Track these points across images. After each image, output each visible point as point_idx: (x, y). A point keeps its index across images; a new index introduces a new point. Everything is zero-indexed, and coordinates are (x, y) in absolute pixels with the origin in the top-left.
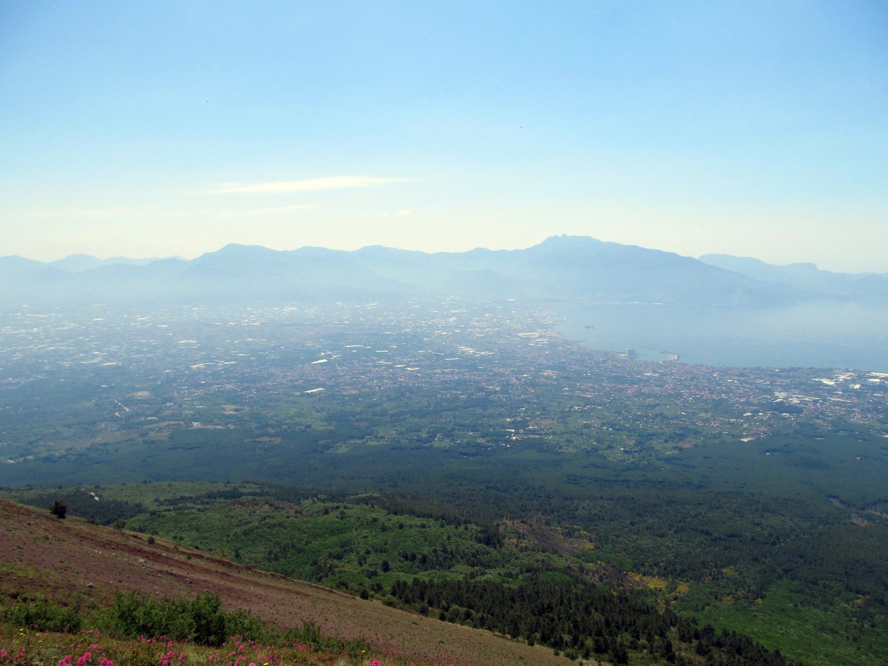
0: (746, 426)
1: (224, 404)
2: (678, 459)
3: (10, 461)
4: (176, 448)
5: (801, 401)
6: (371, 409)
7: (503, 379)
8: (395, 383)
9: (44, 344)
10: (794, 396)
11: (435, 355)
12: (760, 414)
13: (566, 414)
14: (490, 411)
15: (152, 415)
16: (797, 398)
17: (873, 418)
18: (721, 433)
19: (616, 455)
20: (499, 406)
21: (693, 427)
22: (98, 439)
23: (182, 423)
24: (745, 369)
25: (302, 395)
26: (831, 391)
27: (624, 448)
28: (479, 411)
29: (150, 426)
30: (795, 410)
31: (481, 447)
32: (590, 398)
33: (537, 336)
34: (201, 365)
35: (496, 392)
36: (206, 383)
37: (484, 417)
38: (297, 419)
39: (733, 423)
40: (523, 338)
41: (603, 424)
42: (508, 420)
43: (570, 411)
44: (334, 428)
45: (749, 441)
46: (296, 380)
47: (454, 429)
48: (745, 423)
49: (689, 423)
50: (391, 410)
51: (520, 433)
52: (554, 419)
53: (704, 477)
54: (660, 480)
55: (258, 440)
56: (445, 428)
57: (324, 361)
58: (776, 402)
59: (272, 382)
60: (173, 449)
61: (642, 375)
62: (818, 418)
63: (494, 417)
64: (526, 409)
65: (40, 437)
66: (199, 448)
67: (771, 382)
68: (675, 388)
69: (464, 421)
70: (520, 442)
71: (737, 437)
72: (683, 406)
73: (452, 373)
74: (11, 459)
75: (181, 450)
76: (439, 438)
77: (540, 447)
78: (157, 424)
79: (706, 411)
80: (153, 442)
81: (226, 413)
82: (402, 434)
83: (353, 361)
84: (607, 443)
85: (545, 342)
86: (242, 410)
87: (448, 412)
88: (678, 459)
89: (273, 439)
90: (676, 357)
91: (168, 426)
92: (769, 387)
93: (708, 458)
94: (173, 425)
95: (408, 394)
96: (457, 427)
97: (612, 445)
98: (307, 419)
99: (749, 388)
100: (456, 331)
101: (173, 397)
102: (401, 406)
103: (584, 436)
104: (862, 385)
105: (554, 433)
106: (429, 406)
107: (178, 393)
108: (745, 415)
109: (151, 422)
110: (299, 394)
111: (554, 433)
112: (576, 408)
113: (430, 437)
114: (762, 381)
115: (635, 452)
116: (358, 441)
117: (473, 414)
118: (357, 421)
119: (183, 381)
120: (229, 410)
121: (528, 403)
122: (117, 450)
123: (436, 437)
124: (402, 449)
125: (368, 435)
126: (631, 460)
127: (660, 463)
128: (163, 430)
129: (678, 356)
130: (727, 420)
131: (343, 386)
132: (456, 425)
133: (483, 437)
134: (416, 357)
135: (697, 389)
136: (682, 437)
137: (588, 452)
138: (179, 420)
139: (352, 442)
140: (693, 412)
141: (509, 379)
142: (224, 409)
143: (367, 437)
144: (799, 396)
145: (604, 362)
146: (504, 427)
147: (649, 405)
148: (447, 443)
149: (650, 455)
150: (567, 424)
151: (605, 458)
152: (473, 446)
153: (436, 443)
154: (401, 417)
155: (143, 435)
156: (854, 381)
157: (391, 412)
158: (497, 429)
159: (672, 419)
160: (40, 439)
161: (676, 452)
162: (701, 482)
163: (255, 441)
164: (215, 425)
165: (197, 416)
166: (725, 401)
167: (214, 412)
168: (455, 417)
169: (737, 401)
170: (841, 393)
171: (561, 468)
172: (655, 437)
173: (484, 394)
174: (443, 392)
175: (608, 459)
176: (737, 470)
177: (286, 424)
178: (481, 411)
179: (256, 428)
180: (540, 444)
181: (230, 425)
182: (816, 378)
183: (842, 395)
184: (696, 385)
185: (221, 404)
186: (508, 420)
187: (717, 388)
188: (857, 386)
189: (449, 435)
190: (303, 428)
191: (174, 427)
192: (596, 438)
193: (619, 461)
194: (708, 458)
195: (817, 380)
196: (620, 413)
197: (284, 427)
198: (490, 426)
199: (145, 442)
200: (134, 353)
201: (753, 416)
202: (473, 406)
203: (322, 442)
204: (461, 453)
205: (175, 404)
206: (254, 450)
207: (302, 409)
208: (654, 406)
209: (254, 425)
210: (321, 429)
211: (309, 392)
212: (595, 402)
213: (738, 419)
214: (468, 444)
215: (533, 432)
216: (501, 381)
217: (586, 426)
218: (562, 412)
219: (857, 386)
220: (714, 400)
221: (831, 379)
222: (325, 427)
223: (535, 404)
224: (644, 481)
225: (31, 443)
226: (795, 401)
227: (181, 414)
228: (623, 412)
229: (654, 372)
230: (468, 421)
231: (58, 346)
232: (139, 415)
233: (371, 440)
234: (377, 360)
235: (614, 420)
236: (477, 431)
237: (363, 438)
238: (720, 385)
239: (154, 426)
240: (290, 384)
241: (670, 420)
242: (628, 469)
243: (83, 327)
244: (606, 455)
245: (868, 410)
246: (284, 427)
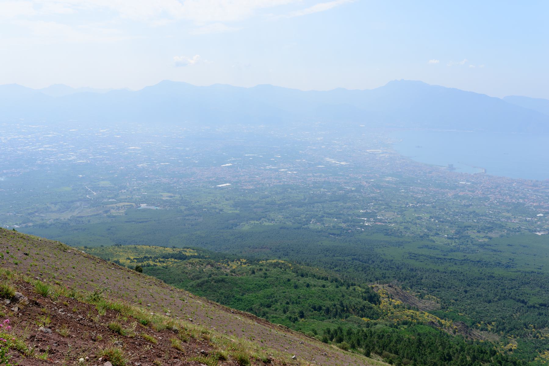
0: (539, 223)
1: (162, 192)
2: (488, 245)
3: (15, 226)
4: (130, 222)
6: (264, 200)
7: (356, 182)
8: (280, 182)
9: (36, 146)
11: (308, 163)
13: (404, 209)
14: (349, 204)
15: (113, 198)
18: (520, 227)
19: (441, 240)
20: (355, 201)
21: (499, 222)
22: (76, 213)
23: (134, 204)
24: (537, 181)
25: (216, 188)
27: (448, 235)
28: (341, 204)
29: (111, 205)
31: (344, 230)
32: (420, 198)
33: (380, 152)
34: (145, 165)
35: (352, 191)
36: (148, 177)
37: (344, 208)
38: (213, 205)
39: (529, 221)
40: (370, 153)
41: (431, 217)
42: (361, 211)
43: (406, 207)
44: (239, 212)
45: (542, 235)
46: (210, 177)
47: (323, 216)
49: (496, 219)
50: (278, 201)
51: (371, 221)
52: (394, 212)
53: (510, 259)
54: (478, 259)
55: (187, 218)
56: (317, 215)
57: (230, 164)
59: (194, 178)
60: (126, 222)
61: (459, 183)
63: (351, 209)
64: (374, 204)
65: (36, 210)
66: (146, 222)
68: (483, 194)
69: (330, 210)
70: (371, 227)
71: (533, 231)
72: (491, 206)
73: (320, 176)
74: (17, 224)
75: (134, 223)
76: (313, 222)
77: (387, 232)
78: (116, 205)
79: (508, 211)
80: (114, 217)
81: (164, 199)
82: (287, 218)
83: (250, 166)
84: (434, 232)
85: (386, 157)
86: (174, 196)
87: (318, 204)
88: (488, 245)
89: (197, 218)
90: (484, 171)
91: (124, 206)
93: (512, 246)
94: (127, 205)
95: (290, 190)
96: (325, 215)
97: (438, 232)
98: (220, 205)
99: (540, 196)
100: (322, 147)
101: (126, 186)
102: (285, 199)
103: (418, 225)
105: (395, 222)
106: (305, 199)
107: (129, 183)
109: (112, 203)
110: (213, 187)
111: (395, 222)
112: (411, 205)
113: (307, 221)
115: (456, 238)
116: (256, 222)
117: (336, 206)
118: (255, 207)
119: (133, 175)
120: (165, 196)
121: (376, 200)
122: (89, 221)
123: (311, 221)
124: (288, 229)
125: (263, 217)
126: (454, 244)
127: (475, 247)
128: (120, 209)
129: (485, 170)
130: (524, 218)
131: (244, 183)
132: (324, 213)
133: (344, 223)
134: (294, 164)
135: (501, 195)
136: (490, 229)
137: (421, 237)
138: (132, 202)
139: (252, 222)
140: (498, 211)
141: (361, 182)
142: (162, 195)
143: (263, 219)
145: (430, 172)
146: (359, 216)
147: (465, 205)
148: (319, 226)
149: (468, 241)
150: (404, 216)
151: (434, 242)
152: (338, 229)
153: (311, 226)
154: (286, 206)
155: (106, 212)
157: (279, 203)
158: (354, 218)
159: (482, 216)
160: (36, 212)
161: (486, 240)
162: (508, 263)
163: (185, 219)
164: (156, 207)
165: (144, 200)
166: (524, 204)
167: (155, 198)
168: (323, 207)
169: (531, 205)
171: (404, 248)
172: (470, 228)
173: (344, 192)
174: (313, 189)
175: (436, 242)
176: (534, 255)
177: (205, 208)
178: (342, 204)
179: (185, 210)
180: (386, 230)
181: (167, 207)
184: (499, 192)
185: (160, 192)
186: (361, 211)
187: (516, 194)
189: (320, 220)
190: (217, 211)
191: (128, 207)
192: (426, 227)
193: (445, 244)
194: (512, 246)
196: (443, 210)
197: (204, 210)
198: (349, 215)
199: (109, 217)
200: (98, 155)
201: (544, 216)
202: (336, 201)
203: (231, 221)
204: (330, 234)
205: (127, 190)
206: (185, 225)
207: (216, 198)
208: (468, 206)
209: (183, 208)
210: (230, 212)
211: (220, 186)
212: (424, 201)
213: (533, 218)
214: (334, 227)
215: (380, 221)
216: (355, 183)
217: (418, 218)
218: (400, 207)
220: (514, 203)
222: (233, 211)
223: (381, 201)
224: (465, 260)
225: (29, 214)
227: (132, 198)
228: (445, 209)
229: (467, 181)
230: (333, 211)
231: (46, 147)
232: (103, 197)
233: (266, 221)
234: (267, 166)
235: (439, 215)
236: (340, 218)
237: (260, 219)
238: (518, 192)
239: (114, 205)
240: (206, 180)
241: (481, 216)
242: (452, 251)
243: (62, 135)
244: (434, 240)
246: (204, 210)
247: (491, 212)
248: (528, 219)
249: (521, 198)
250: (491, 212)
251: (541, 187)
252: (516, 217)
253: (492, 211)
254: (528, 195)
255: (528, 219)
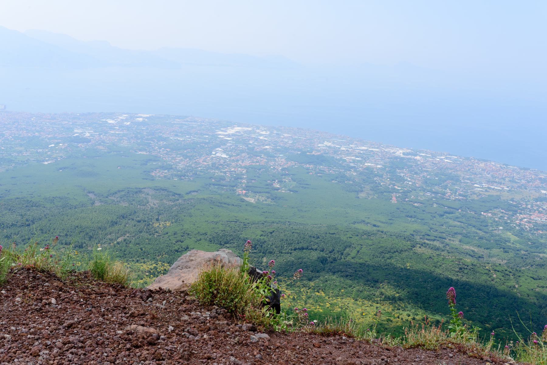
5: (91, 134)
10: (87, 131)
12: (61, 144)
16: (89, 132)
17: (134, 142)
26: (112, 127)
30: (86, 141)
48: (49, 151)
58: (74, 137)
62: (100, 144)
67: (73, 123)
92: (71, 126)
99: (56, 128)
104: (132, 122)
108: (50, 146)
114: (67, 122)
140: (11, 147)
144: (89, 131)
156: (127, 120)
170: (118, 128)
182: (103, 119)
183: (119, 129)
187: (33, 128)
188: (129, 123)
195: (104, 120)
201: (55, 147)
213: (44, 149)
219: (129, 123)
221: (113, 119)
226: (87, 135)
245: (132, 138)
247: (3, 148)
248: (39, 150)
249: (37, 131)
250: (3, 148)
251: (59, 119)
252: (28, 150)
253: (4, 147)
254: (45, 128)
255: (39, 150)
